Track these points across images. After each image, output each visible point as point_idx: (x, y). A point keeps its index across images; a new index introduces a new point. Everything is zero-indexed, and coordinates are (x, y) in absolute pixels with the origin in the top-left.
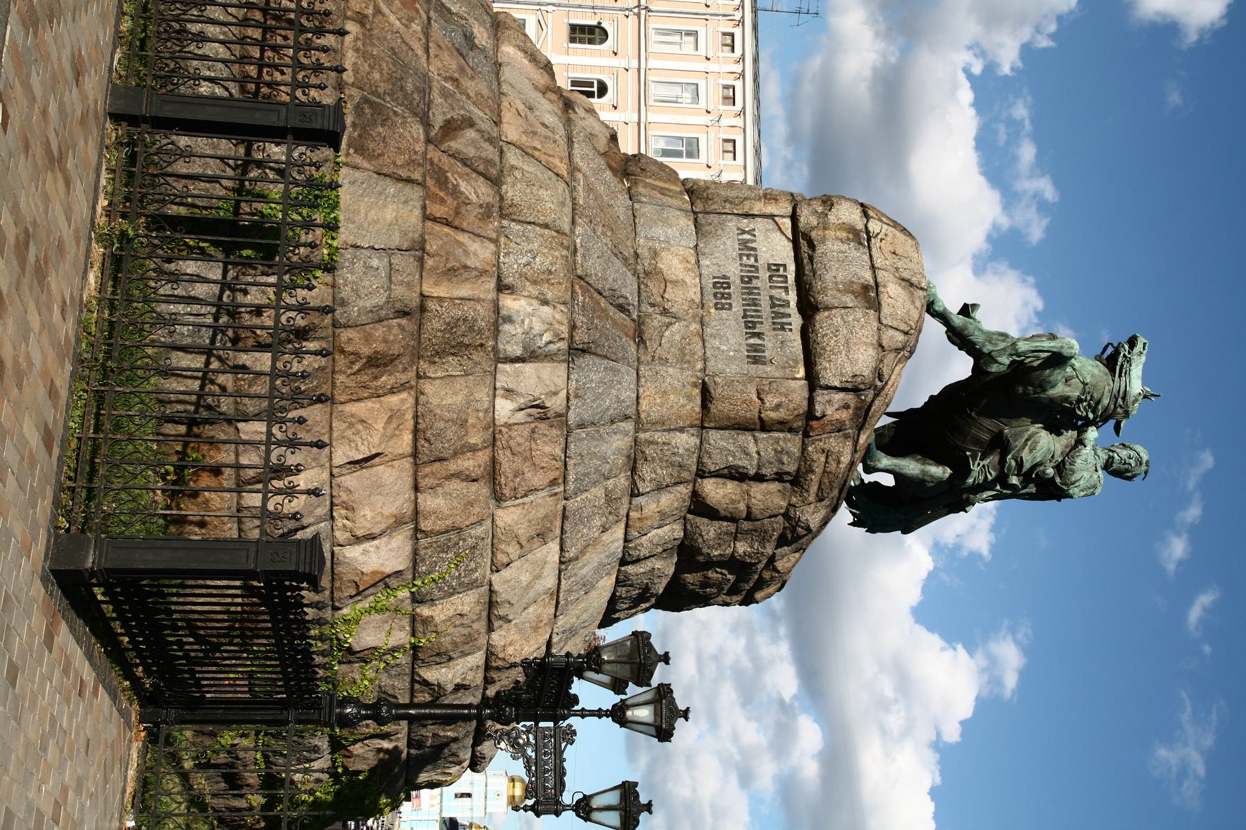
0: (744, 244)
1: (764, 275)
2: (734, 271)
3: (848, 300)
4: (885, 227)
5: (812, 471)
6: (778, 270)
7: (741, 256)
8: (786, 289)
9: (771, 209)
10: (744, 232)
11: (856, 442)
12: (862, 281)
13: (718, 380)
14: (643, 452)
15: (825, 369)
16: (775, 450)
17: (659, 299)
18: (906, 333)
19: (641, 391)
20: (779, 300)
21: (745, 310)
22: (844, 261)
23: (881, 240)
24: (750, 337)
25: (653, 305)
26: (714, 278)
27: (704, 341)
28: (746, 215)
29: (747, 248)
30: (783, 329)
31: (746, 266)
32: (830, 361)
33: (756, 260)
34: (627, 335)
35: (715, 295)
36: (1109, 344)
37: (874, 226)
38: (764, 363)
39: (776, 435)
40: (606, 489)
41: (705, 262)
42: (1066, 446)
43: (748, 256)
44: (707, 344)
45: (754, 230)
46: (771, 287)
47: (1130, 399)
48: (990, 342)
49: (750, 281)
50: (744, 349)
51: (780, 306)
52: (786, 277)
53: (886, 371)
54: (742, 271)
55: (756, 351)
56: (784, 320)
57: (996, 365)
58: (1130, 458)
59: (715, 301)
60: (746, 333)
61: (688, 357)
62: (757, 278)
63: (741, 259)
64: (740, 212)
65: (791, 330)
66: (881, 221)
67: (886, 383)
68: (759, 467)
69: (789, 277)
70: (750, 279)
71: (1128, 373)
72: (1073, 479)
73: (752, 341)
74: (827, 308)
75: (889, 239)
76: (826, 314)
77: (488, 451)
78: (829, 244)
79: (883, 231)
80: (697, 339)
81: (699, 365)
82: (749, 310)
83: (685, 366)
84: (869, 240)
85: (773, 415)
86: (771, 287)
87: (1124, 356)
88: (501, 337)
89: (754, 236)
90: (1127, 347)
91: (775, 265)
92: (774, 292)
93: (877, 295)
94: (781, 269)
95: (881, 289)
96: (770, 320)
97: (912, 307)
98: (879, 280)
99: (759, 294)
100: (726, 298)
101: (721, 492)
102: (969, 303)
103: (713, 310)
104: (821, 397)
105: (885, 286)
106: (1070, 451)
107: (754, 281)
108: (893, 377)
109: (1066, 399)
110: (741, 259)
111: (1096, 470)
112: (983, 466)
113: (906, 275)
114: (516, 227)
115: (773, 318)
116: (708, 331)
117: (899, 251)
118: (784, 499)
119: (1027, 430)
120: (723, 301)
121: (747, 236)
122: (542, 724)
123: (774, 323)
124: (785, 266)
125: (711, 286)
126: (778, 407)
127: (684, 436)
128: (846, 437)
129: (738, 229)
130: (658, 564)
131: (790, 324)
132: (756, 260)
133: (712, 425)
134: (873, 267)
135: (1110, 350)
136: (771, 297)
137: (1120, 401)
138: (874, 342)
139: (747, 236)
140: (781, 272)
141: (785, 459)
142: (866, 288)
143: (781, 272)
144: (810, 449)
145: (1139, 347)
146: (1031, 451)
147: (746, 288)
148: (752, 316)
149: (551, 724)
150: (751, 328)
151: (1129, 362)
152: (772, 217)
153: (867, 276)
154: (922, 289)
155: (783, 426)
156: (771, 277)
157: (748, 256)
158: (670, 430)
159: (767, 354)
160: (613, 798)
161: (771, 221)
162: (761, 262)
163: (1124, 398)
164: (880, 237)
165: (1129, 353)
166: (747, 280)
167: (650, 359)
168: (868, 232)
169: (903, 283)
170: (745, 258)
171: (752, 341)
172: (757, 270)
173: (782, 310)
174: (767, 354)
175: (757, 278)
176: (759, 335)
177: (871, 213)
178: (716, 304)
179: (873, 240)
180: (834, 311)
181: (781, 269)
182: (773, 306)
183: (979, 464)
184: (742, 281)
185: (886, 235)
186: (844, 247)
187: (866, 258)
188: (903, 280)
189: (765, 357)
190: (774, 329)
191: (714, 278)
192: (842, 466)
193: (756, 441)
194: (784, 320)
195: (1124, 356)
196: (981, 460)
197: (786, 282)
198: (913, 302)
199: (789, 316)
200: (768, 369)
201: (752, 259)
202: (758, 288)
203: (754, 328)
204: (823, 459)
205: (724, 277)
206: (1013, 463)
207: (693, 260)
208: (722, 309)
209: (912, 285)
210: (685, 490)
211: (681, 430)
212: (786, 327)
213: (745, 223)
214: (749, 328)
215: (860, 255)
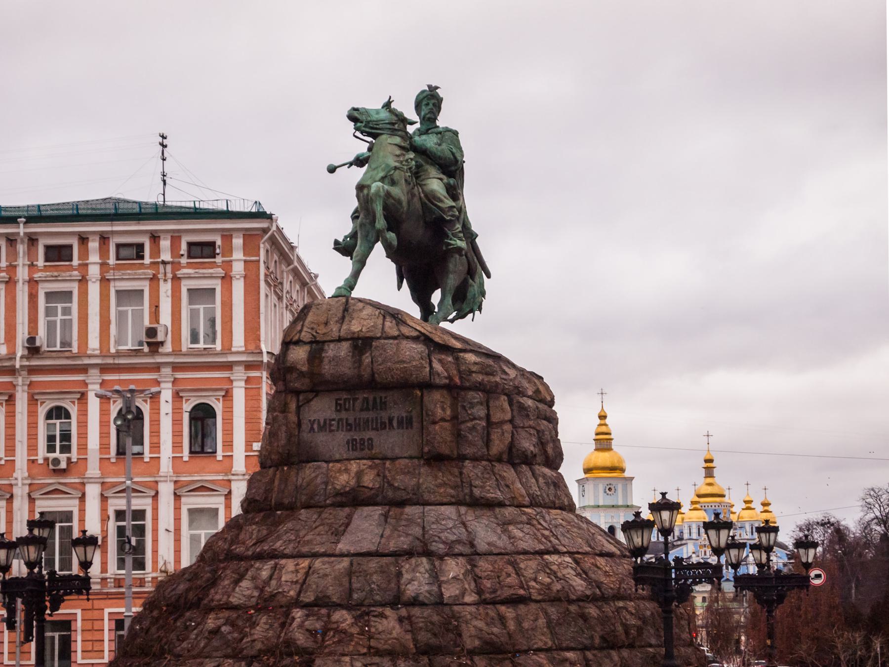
0: (322, 428)
1: (344, 415)
2: (342, 437)
3: (367, 359)
4: (305, 329)
5: (483, 380)
6: (340, 405)
7: (331, 431)
8: (355, 400)
9: (293, 406)
10: (312, 429)
11: (461, 351)
12: (351, 350)
13: (426, 449)
14: (477, 499)
15: (417, 377)
16: (470, 408)
17: (373, 492)
18: (384, 317)
19: (437, 502)
20: (363, 404)
21: (373, 429)
22: (335, 359)
23: (316, 332)
24: (393, 426)
25: (377, 496)
26: (349, 450)
27: (397, 458)
28: (299, 424)
29: (326, 426)
30: (385, 403)
31: (338, 427)
32: (411, 375)
33: (334, 420)
34: (402, 514)
35: (362, 450)
36: (354, 136)
37: (306, 336)
38: (411, 418)
39: (460, 409)
40: (504, 524)
41: (337, 457)
42: (427, 163)
43: (331, 425)
44: (400, 455)
45: (310, 420)
46: (354, 410)
47: (394, 118)
48: (367, 236)
49: (350, 425)
50: (401, 431)
51: (367, 403)
52: (345, 399)
53: (415, 334)
54: (342, 430)
55: (402, 422)
56: (378, 401)
57: (393, 243)
58: (427, 104)
59: (367, 450)
60: (389, 429)
61: (411, 470)
62: (347, 419)
63: (333, 431)
64: (297, 431)
65: (386, 398)
66: (301, 331)
67: (423, 334)
68: (480, 419)
69: (345, 397)
70: (348, 424)
71: (377, 122)
72: (452, 157)
73: (395, 424)
74: (373, 375)
75: (315, 326)
76: (376, 375)
77: (498, 606)
78: (323, 371)
79: (309, 331)
80: (397, 462)
81: (416, 461)
82: (372, 426)
83: (417, 472)
84: (317, 342)
85: (448, 412)
86: (354, 410)
87: (364, 127)
88: (426, 601)
89: (315, 420)
90: (359, 124)
91: (336, 406)
92: (358, 408)
93: (358, 338)
94: (339, 402)
95: (356, 335)
96: (378, 412)
97: (365, 312)
98: (349, 337)
99: (360, 419)
100: (364, 443)
101: (497, 442)
102: (333, 246)
103: (374, 452)
104: (437, 381)
105: (354, 333)
106: (430, 159)
107: (350, 422)
108: (418, 328)
109: (406, 180)
110: (333, 431)
111: (440, 133)
112: (452, 234)
113: (340, 315)
114: (355, 596)
115: (377, 409)
116: (389, 455)
117: (323, 319)
118: (498, 399)
119: (426, 204)
120: (366, 444)
121: (315, 426)
122: (673, 576)
123: (381, 409)
124: (337, 400)
125: (355, 452)
126: (443, 409)
127: (464, 471)
128: (457, 359)
129: (310, 432)
130: (541, 480)
131: (381, 398)
132: (334, 420)
133: (455, 453)
134: (340, 340)
135: (358, 134)
136: (362, 410)
137: (396, 126)
138: (396, 342)
139: (315, 426)
140: (342, 402)
141: (476, 401)
142: (355, 347)
143: (342, 402)
144: (468, 384)
145: (356, 114)
146: (441, 201)
147: (355, 428)
148: (377, 425)
149: (673, 570)
150: (384, 426)
151: (368, 122)
152: (299, 407)
153: (346, 345)
154: (347, 301)
155: (454, 407)
156: (346, 410)
157: (331, 425)
158: (462, 482)
159: (404, 415)
160: (712, 533)
161: (302, 408)
162: (334, 416)
163: (393, 124)
164: (315, 334)
165: (362, 122)
166: (349, 427)
167: (414, 497)
168: (311, 343)
169: (347, 319)
170: (333, 428)
171: (395, 424)
172: (340, 420)
173: (371, 403)
174: (404, 415)
175: (347, 419)
176: (391, 420)
177: (296, 338)
178: (369, 449)
179: (318, 339)
180: (375, 370)
181: (339, 402)
182: (367, 409)
183: (451, 239)
184: (350, 430)
185: (312, 329)
186: (326, 361)
187: (332, 345)
188: (343, 318)
189: (407, 417)
190: (386, 409)
191: (349, 450)
192: (478, 360)
193: (463, 422)
194: (378, 401)
195: (364, 127)
196: (448, 237)
197: (349, 399)
198: (361, 310)
199: (375, 399)
200: (414, 414)
201: (333, 422)
202: (355, 419)
203: (385, 423)
204: (474, 375)
205: (348, 443)
206: (450, 213)
207: (338, 465)
208: (372, 445)
209: (346, 310)
210: (498, 467)
211: (461, 473)
212: (383, 400)
213: (305, 426)
214: (385, 426)
215: (331, 351)
